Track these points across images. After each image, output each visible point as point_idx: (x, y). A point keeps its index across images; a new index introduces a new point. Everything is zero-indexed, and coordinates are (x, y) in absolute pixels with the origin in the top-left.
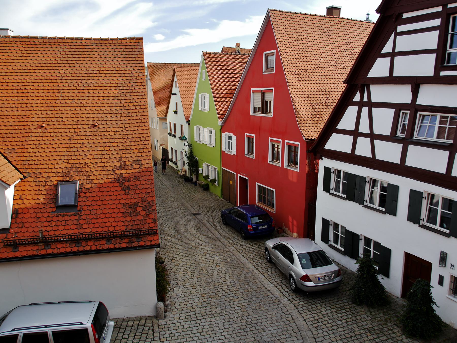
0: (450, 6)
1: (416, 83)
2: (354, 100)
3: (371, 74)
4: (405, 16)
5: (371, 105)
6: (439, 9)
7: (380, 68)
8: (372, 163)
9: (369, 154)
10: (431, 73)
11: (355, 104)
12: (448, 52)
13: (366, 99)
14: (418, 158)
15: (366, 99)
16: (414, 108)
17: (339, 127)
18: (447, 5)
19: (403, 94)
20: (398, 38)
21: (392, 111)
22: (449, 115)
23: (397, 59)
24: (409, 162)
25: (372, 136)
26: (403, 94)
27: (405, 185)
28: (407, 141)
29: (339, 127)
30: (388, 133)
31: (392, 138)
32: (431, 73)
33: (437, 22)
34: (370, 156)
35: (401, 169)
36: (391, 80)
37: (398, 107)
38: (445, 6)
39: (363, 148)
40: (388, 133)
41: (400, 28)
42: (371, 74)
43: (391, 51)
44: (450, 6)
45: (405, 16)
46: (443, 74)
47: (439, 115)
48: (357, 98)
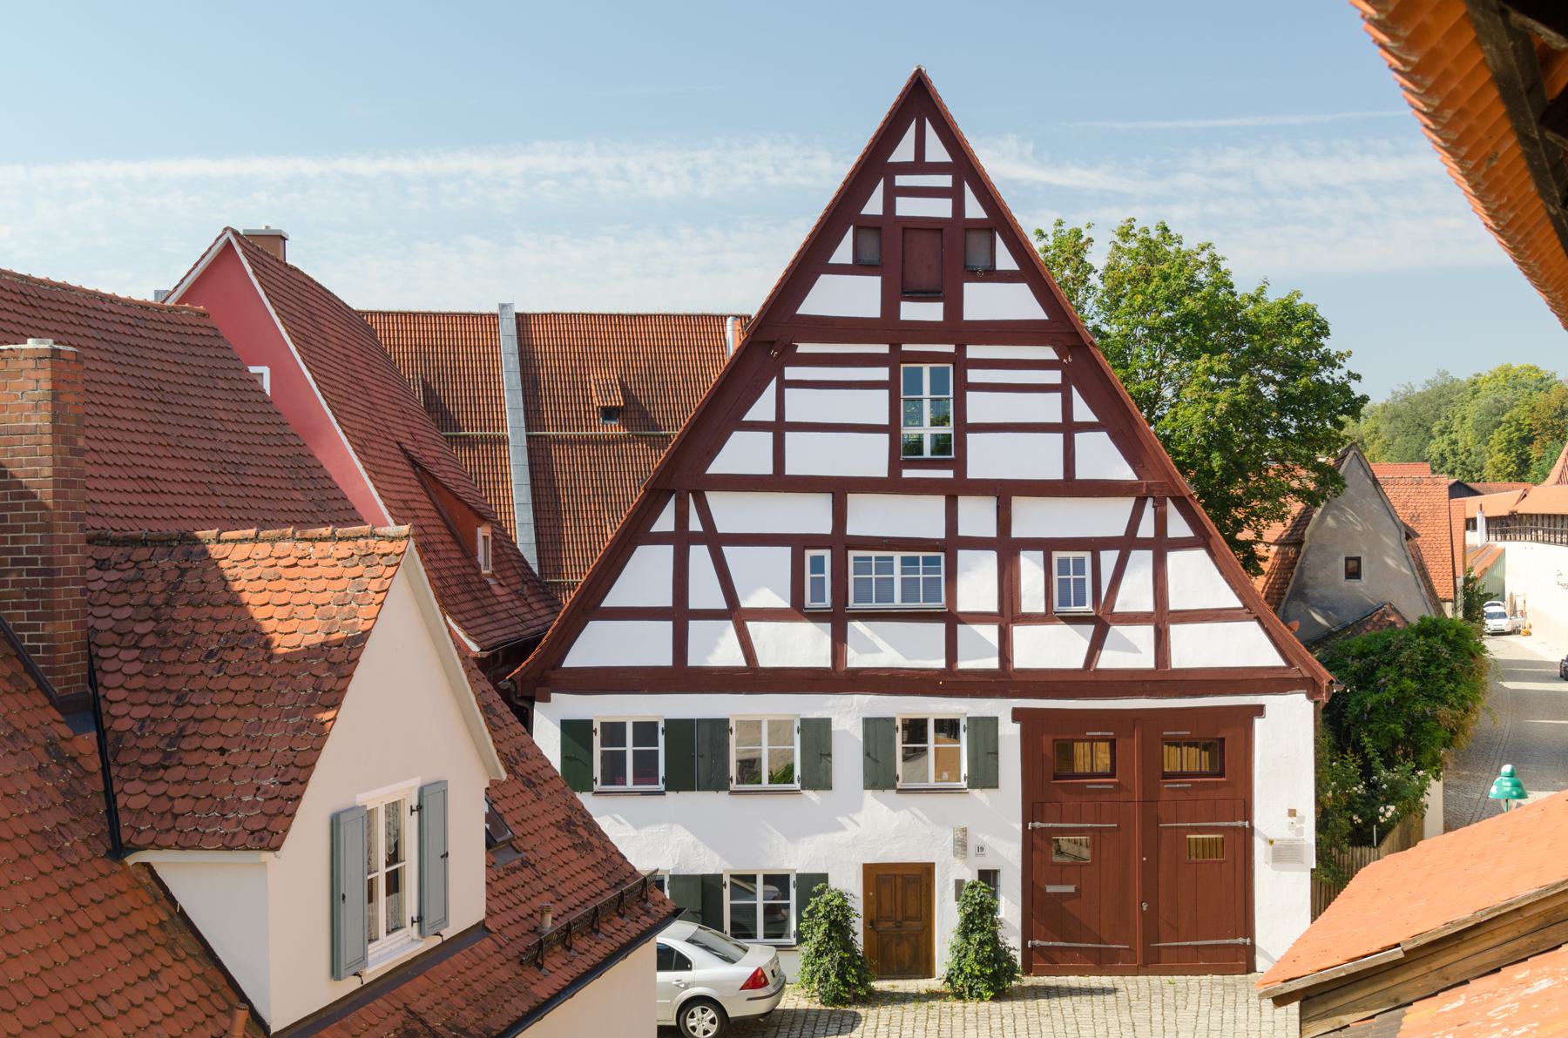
1: (839, 489)
3: (718, 467)
4: (803, 348)
5: (716, 541)
6: (884, 349)
9: (741, 662)
11: (661, 539)
13: (695, 525)
15: (695, 525)
16: (839, 542)
19: (813, 515)
21: (785, 553)
22: (921, 554)
26: (813, 515)
27: (848, 715)
31: (798, 610)
32: (883, 472)
33: (882, 374)
34: (741, 662)
35: (837, 679)
36: (779, 481)
37: (799, 543)
39: (716, 647)
41: (791, 373)
43: (771, 416)
45: (803, 348)
48: (665, 522)
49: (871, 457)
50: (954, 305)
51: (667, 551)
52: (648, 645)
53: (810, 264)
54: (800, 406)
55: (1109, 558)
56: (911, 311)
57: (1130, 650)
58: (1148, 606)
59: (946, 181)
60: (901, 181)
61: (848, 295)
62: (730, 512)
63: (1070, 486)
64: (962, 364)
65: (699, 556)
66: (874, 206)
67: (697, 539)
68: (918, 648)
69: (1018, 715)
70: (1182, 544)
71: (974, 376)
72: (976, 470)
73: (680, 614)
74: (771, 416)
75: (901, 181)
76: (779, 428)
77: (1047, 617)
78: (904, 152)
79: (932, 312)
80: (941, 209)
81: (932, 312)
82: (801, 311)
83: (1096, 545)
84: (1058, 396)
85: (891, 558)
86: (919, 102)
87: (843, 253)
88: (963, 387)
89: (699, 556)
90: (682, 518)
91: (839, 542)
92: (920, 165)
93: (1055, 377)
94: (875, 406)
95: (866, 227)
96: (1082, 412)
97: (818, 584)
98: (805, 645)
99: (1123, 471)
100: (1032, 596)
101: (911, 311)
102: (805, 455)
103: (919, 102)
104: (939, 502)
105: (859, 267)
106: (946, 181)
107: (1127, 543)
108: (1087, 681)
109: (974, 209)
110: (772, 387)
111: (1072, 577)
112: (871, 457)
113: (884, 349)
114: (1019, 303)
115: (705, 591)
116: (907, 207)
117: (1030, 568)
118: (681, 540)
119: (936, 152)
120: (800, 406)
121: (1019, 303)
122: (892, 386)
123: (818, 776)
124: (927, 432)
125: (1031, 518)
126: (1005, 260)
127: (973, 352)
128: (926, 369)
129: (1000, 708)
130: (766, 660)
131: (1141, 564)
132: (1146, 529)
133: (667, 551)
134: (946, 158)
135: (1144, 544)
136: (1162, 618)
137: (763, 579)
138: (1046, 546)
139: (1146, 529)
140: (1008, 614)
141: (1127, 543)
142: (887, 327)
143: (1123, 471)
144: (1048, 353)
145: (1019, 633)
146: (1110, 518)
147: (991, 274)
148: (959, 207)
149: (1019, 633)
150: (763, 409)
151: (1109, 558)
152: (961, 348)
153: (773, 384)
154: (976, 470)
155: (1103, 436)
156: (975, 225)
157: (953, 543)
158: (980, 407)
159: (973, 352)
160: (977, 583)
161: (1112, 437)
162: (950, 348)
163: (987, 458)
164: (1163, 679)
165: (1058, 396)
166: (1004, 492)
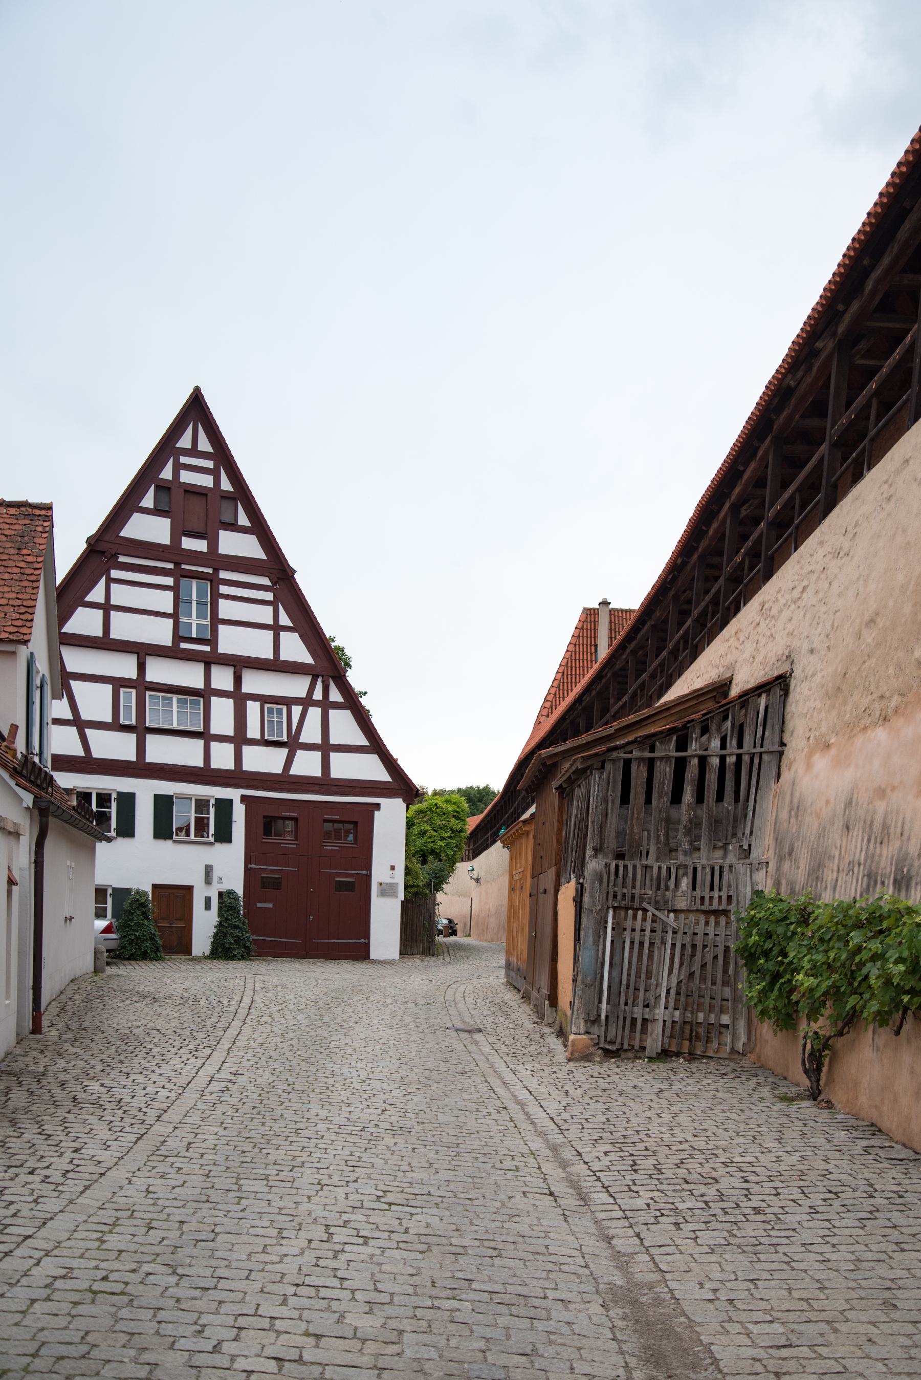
0: (183, 566)
1: (143, 652)
4: (122, 559)
9: (81, 753)
14: (161, 751)
16: (141, 685)
18: (180, 564)
19: (126, 667)
20: (113, 586)
21: (109, 687)
24: (150, 758)
26: (126, 667)
31: (115, 726)
33: (169, 581)
34: (81, 753)
36: (105, 643)
38: (177, 564)
41: (115, 574)
44: (183, 566)
45: (122, 559)
46: (183, 645)
47: (175, 698)
50: (214, 544)
54: (120, 596)
55: (297, 710)
56: (188, 543)
57: (307, 765)
58: (318, 740)
59: (210, 464)
60: (184, 460)
61: (149, 528)
63: (276, 666)
64: (215, 581)
66: (167, 473)
68: (188, 753)
69: (244, 799)
70: (337, 706)
71: (224, 589)
72: (222, 649)
75: (184, 460)
78: (185, 442)
79: (200, 546)
80: (206, 481)
81: (200, 546)
82: (123, 533)
83: (289, 702)
84: (269, 609)
87: (148, 501)
88: (216, 596)
93: (269, 596)
94: (164, 601)
96: (284, 620)
99: (307, 659)
100: (253, 731)
101: (188, 543)
102: (124, 627)
105: (157, 511)
106: (210, 464)
107: (307, 702)
108: (285, 781)
109: (226, 485)
116: (187, 477)
120: (120, 596)
122: (175, 589)
123: (127, 829)
125: (253, 683)
126: (243, 520)
127: (223, 575)
129: (234, 794)
130: (97, 753)
131: (314, 713)
135: (316, 704)
136: (326, 748)
137: (95, 702)
139: (318, 695)
140: (239, 739)
141: (307, 702)
143: (307, 659)
144: (266, 581)
145: (246, 749)
146: (297, 687)
147: (233, 526)
148: (217, 481)
149: (246, 749)
150: (97, 594)
151: (297, 710)
152: (216, 570)
154: (222, 649)
155: (296, 635)
156: (225, 496)
158: (226, 609)
159: (223, 575)
160: (222, 716)
161: (301, 637)
162: (210, 571)
163: (231, 641)
164: (325, 783)
166: (240, 664)
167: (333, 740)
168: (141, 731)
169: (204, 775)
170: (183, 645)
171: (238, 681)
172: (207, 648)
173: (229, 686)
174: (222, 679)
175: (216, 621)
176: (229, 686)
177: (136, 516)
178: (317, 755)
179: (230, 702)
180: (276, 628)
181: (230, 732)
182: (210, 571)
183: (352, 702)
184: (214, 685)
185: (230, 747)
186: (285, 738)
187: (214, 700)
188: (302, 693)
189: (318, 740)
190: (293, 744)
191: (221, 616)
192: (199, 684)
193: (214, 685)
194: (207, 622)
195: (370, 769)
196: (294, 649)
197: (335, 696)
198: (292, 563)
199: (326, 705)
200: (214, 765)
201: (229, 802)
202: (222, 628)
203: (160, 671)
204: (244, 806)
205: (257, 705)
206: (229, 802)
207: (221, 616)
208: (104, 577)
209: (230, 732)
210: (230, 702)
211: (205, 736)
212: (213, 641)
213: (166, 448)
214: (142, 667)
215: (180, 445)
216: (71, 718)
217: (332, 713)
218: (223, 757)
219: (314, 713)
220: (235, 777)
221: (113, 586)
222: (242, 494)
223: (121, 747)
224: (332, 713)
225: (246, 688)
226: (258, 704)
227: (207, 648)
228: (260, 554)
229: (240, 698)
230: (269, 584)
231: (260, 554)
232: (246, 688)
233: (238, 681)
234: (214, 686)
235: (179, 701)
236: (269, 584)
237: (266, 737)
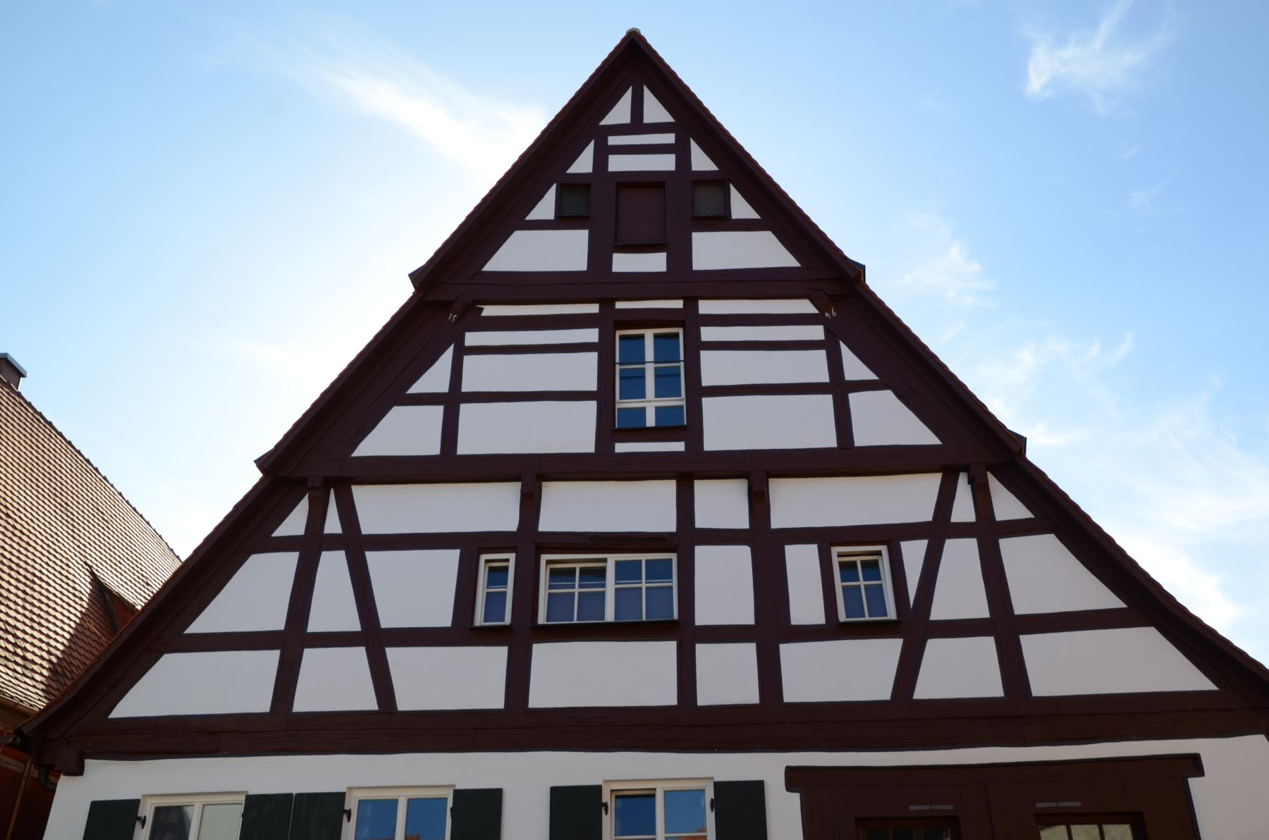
0: (620, 305)
1: (531, 473)
2: (281, 532)
3: (368, 447)
4: (489, 311)
5: (357, 545)
6: (593, 308)
7: (405, 431)
8: (387, 729)
9: (368, 702)
10: (586, 444)
12: (618, 406)
13: (333, 525)
14: (568, 675)
15: (333, 525)
16: (529, 541)
17: (203, 624)
19: (494, 508)
20: (468, 360)
23: (466, 409)
24: (541, 696)
25: (374, 638)
26: (494, 508)
28: (520, 638)
29: (199, 626)
30: (443, 617)
31: (462, 632)
32: (586, 444)
33: (591, 335)
34: (368, 702)
35: (516, 726)
36: (449, 467)
37: (470, 546)
39: (335, 682)
40: (443, 617)
41: (472, 339)
42: (368, 447)
43: (444, 387)
44: (620, 305)
45: (489, 311)
46: (621, 448)
47: (612, 560)
48: (295, 524)
49: (574, 430)
50: (681, 255)
51: (290, 560)
52: (243, 685)
53: (501, 212)
54: (480, 373)
55: (914, 553)
56: (624, 263)
57: (960, 671)
58: (979, 609)
59: (669, 138)
60: (613, 140)
62: (379, 508)
63: (847, 460)
64: (691, 321)
65: (333, 565)
66: (583, 164)
67: (333, 543)
68: (637, 675)
69: (794, 778)
70: (1016, 528)
71: (708, 334)
72: (712, 442)
73: (292, 640)
74: (444, 387)
75: (613, 140)
76: (452, 400)
77: (832, 630)
78: (620, 113)
79: (656, 262)
80: (666, 163)
81: (656, 262)
82: (491, 266)
83: (892, 535)
84: (821, 355)
85: (605, 560)
86: (633, 64)
87: (545, 208)
88: (695, 346)
89: (333, 565)
90: (317, 518)
91: (529, 541)
92: (637, 124)
93: (816, 332)
94: (582, 371)
95: (572, 188)
96: (855, 368)
97: (495, 602)
98: (469, 679)
100: (806, 606)
101: (624, 263)
103: (633, 64)
104: (668, 489)
105: (563, 220)
106: (669, 138)
107: (938, 530)
108: (903, 718)
109: (701, 161)
110: (448, 355)
111: (862, 583)
112: (574, 430)
113: (593, 308)
114: (765, 251)
115: (333, 607)
117: (802, 564)
118: (310, 548)
119: (655, 111)
120: (480, 373)
121: (765, 251)
122: (603, 349)
124: (650, 405)
126: (740, 208)
127: (706, 307)
128: (649, 334)
129: (766, 768)
130: (406, 701)
132: (964, 510)
133: (290, 560)
134: (666, 117)
135: (962, 531)
136: (1005, 626)
137: (417, 589)
138: (824, 538)
139: (964, 510)
140: (771, 628)
141: (938, 530)
142: (596, 282)
145: (788, 652)
146: (911, 498)
149: (788, 652)
150: (435, 379)
151: (914, 553)
152: (691, 302)
153: (450, 352)
154: (712, 442)
155: (888, 394)
156: (703, 179)
157: (687, 537)
158: (715, 367)
160: (723, 586)
161: (900, 396)
162: (678, 304)
164: (1017, 713)
165: (821, 355)
166: (758, 470)
167: (1022, 605)
168: (520, 638)
169: (685, 725)
170: (621, 448)
171: (759, 503)
172: (679, 446)
173: (741, 521)
174: (721, 504)
175: (697, 392)
176: (741, 521)
177: (518, 236)
178: (986, 646)
179: (741, 556)
180: (839, 388)
181: (747, 617)
182: (678, 304)
183: (1057, 514)
184: (703, 520)
185: (747, 652)
186: (892, 614)
187: (703, 554)
188: (924, 513)
189: (979, 609)
190: (915, 627)
191: (707, 380)
192: (668, 524)
193: (703, 520)
194: (679, 401)
195: (1145, 664)
196: (885, 419)
197: (1008, 506)
198: (852, 253)
199: (988, 532)
200: (707, 696)
201: (755, 791)
202: (707, 402)
203: (569, 508)
204: (795, 798)
205: (812, 551)
206: (755, 791)
207: (707, 380)
208: (451, 348)
209: (747, 617)
210: (741, 556)
211: (685, 633)
212: (691, 428)
213: (578, 122)
214: (530, 505)
215: (606, 121)
216: (356, 627)
217: (1008, 546)
218: (728, 677)
219: (961, 555)
220: (769, 722)
221: (468, 360)
222: (739, 168)
223: (474, 680)
224: (1008, 546)
225: (780, 519)
226: (812, 551)
227: (679, 446)
228: (786, 259)
229: (766, 543)
230: (815, 311)
231: (786, 259)
232: (780, 519)
233: (759, 503)
234: (700, 522)
235: (625, 571)
236: (815, 311)
237: (842, 617)
